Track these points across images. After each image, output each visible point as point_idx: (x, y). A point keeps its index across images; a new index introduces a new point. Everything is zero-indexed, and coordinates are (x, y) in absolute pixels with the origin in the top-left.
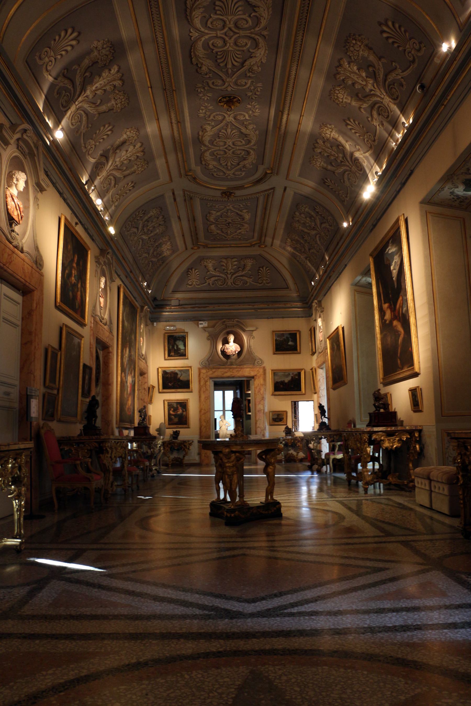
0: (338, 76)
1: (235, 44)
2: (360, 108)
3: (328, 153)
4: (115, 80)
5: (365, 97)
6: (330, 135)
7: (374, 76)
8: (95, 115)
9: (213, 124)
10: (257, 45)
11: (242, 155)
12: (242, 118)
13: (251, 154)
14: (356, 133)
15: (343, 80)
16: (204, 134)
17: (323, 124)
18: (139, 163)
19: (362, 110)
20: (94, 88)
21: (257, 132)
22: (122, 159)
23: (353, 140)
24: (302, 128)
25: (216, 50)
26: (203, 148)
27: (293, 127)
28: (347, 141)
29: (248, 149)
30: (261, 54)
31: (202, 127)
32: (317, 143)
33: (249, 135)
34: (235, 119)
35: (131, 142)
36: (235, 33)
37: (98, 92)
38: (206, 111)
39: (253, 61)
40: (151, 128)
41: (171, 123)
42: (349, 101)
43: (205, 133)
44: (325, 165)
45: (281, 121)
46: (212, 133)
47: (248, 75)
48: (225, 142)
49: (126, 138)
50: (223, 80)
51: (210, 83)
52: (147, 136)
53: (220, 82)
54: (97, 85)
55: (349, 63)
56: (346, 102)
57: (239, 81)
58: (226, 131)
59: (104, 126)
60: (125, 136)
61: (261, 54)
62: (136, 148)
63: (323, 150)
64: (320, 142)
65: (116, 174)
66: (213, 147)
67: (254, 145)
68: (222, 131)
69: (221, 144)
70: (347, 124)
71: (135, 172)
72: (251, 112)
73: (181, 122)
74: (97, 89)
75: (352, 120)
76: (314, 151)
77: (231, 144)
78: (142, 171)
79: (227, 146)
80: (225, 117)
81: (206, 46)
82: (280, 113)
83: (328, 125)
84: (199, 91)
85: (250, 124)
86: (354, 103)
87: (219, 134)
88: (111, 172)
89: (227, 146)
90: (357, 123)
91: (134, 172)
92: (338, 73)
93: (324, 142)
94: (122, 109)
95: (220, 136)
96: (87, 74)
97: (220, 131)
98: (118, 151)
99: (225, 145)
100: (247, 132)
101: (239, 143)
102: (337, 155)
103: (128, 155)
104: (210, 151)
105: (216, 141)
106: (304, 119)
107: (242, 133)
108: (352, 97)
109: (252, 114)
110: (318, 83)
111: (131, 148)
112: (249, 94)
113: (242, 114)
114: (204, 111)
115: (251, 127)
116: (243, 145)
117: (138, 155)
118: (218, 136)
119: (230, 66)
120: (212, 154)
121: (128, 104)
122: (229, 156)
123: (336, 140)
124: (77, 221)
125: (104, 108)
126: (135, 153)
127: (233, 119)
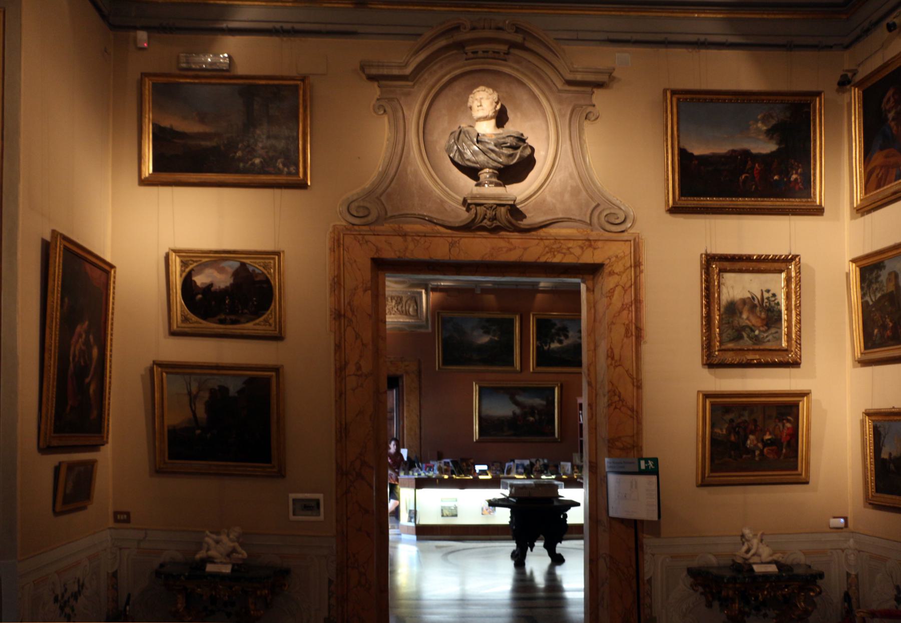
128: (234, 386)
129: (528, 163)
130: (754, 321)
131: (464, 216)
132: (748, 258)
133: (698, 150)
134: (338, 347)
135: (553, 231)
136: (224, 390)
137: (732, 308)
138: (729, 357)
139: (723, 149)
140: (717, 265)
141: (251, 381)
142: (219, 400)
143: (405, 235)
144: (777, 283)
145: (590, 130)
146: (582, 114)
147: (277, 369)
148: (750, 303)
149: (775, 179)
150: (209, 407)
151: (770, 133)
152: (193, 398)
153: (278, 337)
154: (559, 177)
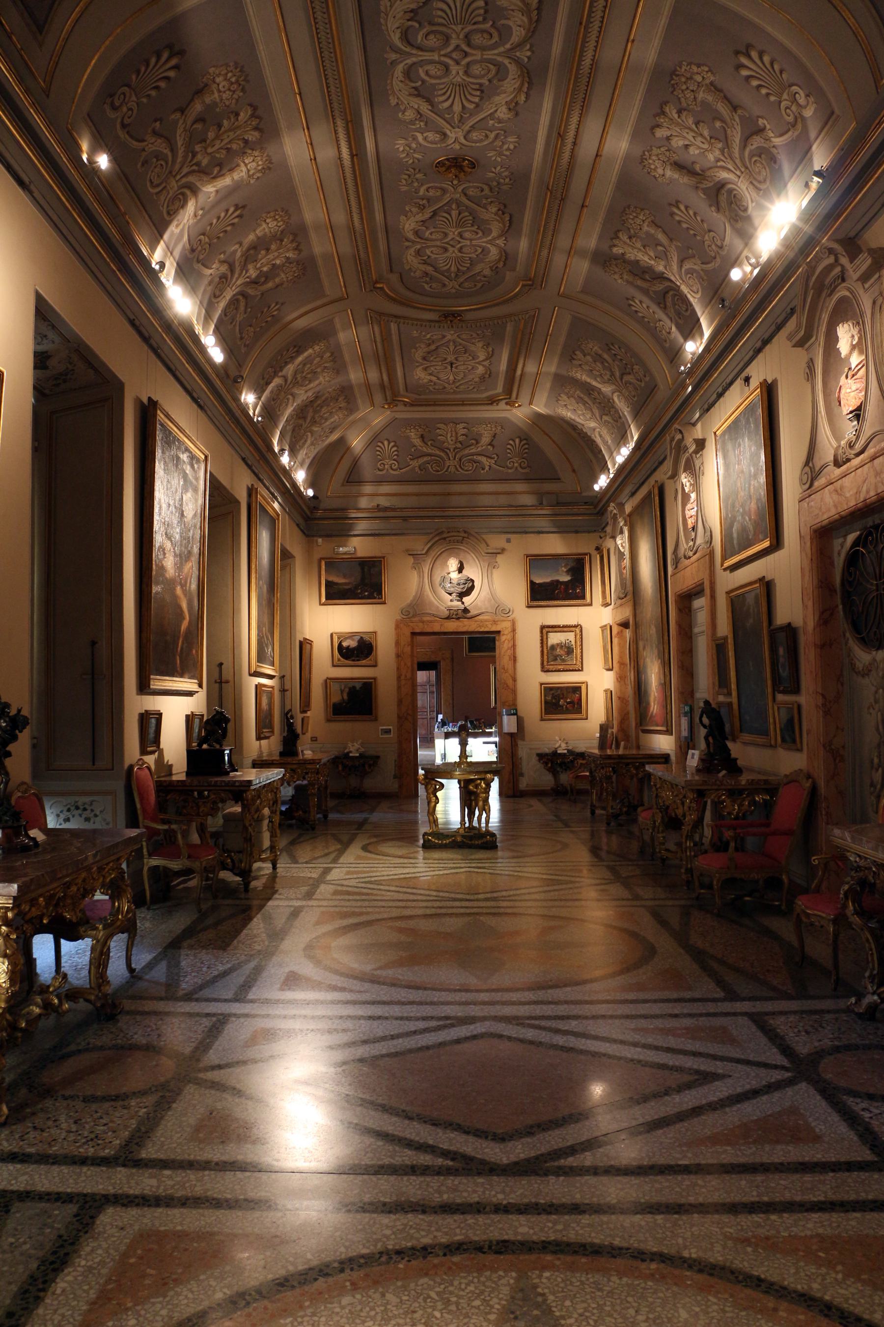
0: (291, 238)
1: (446, 235)
2: (241, 244)
3: (225, 132)
4: (625, 243)
5: (246, 260)
6: (246, 165)
7: (255, 282)
8: (676, 247)
9: (491, 122)
10: (416, 233)
11: (425, 31)
12: (430, 135)
13: (398, 35)
14: (219, 218)
15: (282, 241)
16: (515, 97)
17: (270, 168)
18: (689, 95)
19: (237, 246)
20: (653, 262)
21: (393, 102)
22: (706, 146)
23: (213, 207)
24: (301, 137)
25: (475, 228)
26: (524, 54)
27: (321, 132)
28: (217, 191)
29: (408, 49)
30: (409, 225)
31: (517, 114)
32: (256, 129)
33: (410, 95)
34: (445, 135)
35: (667, 153)
36: (447, 243)
37: (652, 254)
38: (501, 147)
39: (420, 217)
40: (619, 145)
41: (575, 144)
42: (257, 232)
43: (512, 100)
44: (208, 100)
45: (349, 142)
46: (497, 99)
47: (425, 202)
48: (466, 73)
49: (668, 167)
50: (465, 195)
51: (487, 191)
52: (635, 136)
53: (470, 192)
54: (646, 259)
55: (288, 258)
56: (260, 225)
57: (438, 194)
58: (463, 107)
59: (679, 222)
60: (669, 173)
61: (409, 225)
62: (669, 133)
63: (238, 127)
64: (252, 136)
65: (737, 140)
66: (499, 59)
67: (394, 63)
68: (472, 106)
69: (476, 70)
70: (237, 207)
71: (712, 83)
72: (414, 146)
73: (558, 134)
74: (651, 258)
75: (236, 220)
76: (251, 105)
77: (454, 69)
78: (699, 66)
79: (464, 62)
80: (465, 138)
81: (486, 232)
82: (357, 153)
83: (259, 175)
84: (507, 180)
85: (412, 122)
86: (251, 237)
87: (481, 98)
88: (738, 161)
89: (464, 62)
90: (229, 228)
91: (714, 88)
92: (292, 241)
93: (246, 142)
94: (642, 210)
95: (478, 93)
96: (647, 277)
97: (477, 105)
98: (697, 168)
99: (468, 65)
100: (416, 102)
101: (433, 70)
102: (210, 150)
103: (690, 136)
104: (508, 46)
105: (490, 76)
106: (306, 154)
107: (429, 101)
108: (258, 238)
109: (409, 139)
110: (312, 213)
111: (678, 143)
112: (419, 176)
113: (431, 143)
114: (506, 147)
115: (410, 115)
116: (422, 63)
117: (676, 116)
118: (482, 91)
119: (454, 213)
120: (504, 33)
121: (629, 207)
122: (458, 28)
123: (231, 170)
124: (739, 382)
125: (661, 236)
126: (678, 124)
127: (448, 132)
128: (358, 686)
129: (473, 587)
130: (562, 652)
131: (447, 613)
132: (559, 626)
133: (538, 580)
134: (398, 669)
135: (480, 617)
136: (354, 687)
137: (553, 647)
138: (551, 667)
139: (548, 580)
140: (546, 630)
141: (365, 684)
142: (352, 692)
143: (423, 622)
144: (571, 637)
145: (496, 574)
146: (492, 566)
147: (375, 679)
148: (560, 645)
149: (572, 590)
150: (349, 694)
151: (568, 572)
152: (342, 691)
153: (375, 666)
154: (483, 594)
